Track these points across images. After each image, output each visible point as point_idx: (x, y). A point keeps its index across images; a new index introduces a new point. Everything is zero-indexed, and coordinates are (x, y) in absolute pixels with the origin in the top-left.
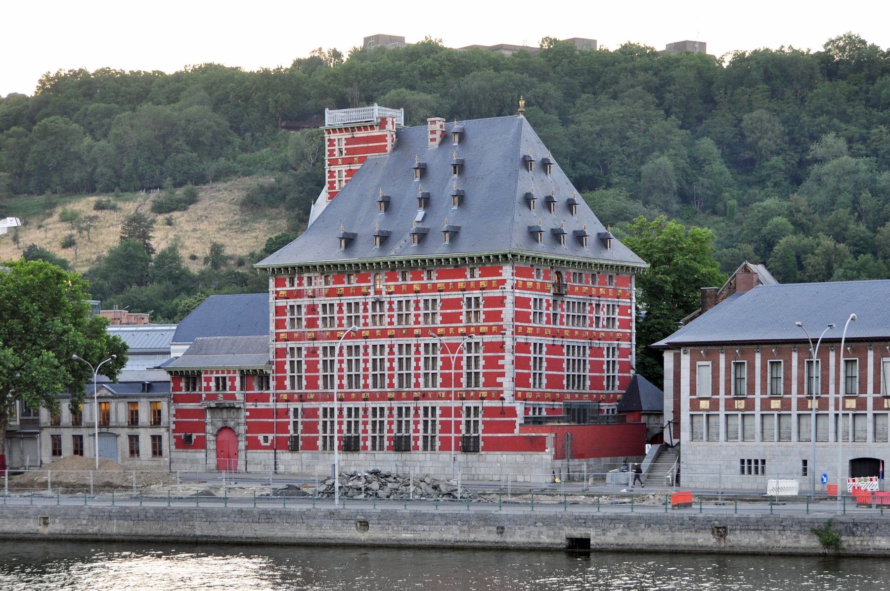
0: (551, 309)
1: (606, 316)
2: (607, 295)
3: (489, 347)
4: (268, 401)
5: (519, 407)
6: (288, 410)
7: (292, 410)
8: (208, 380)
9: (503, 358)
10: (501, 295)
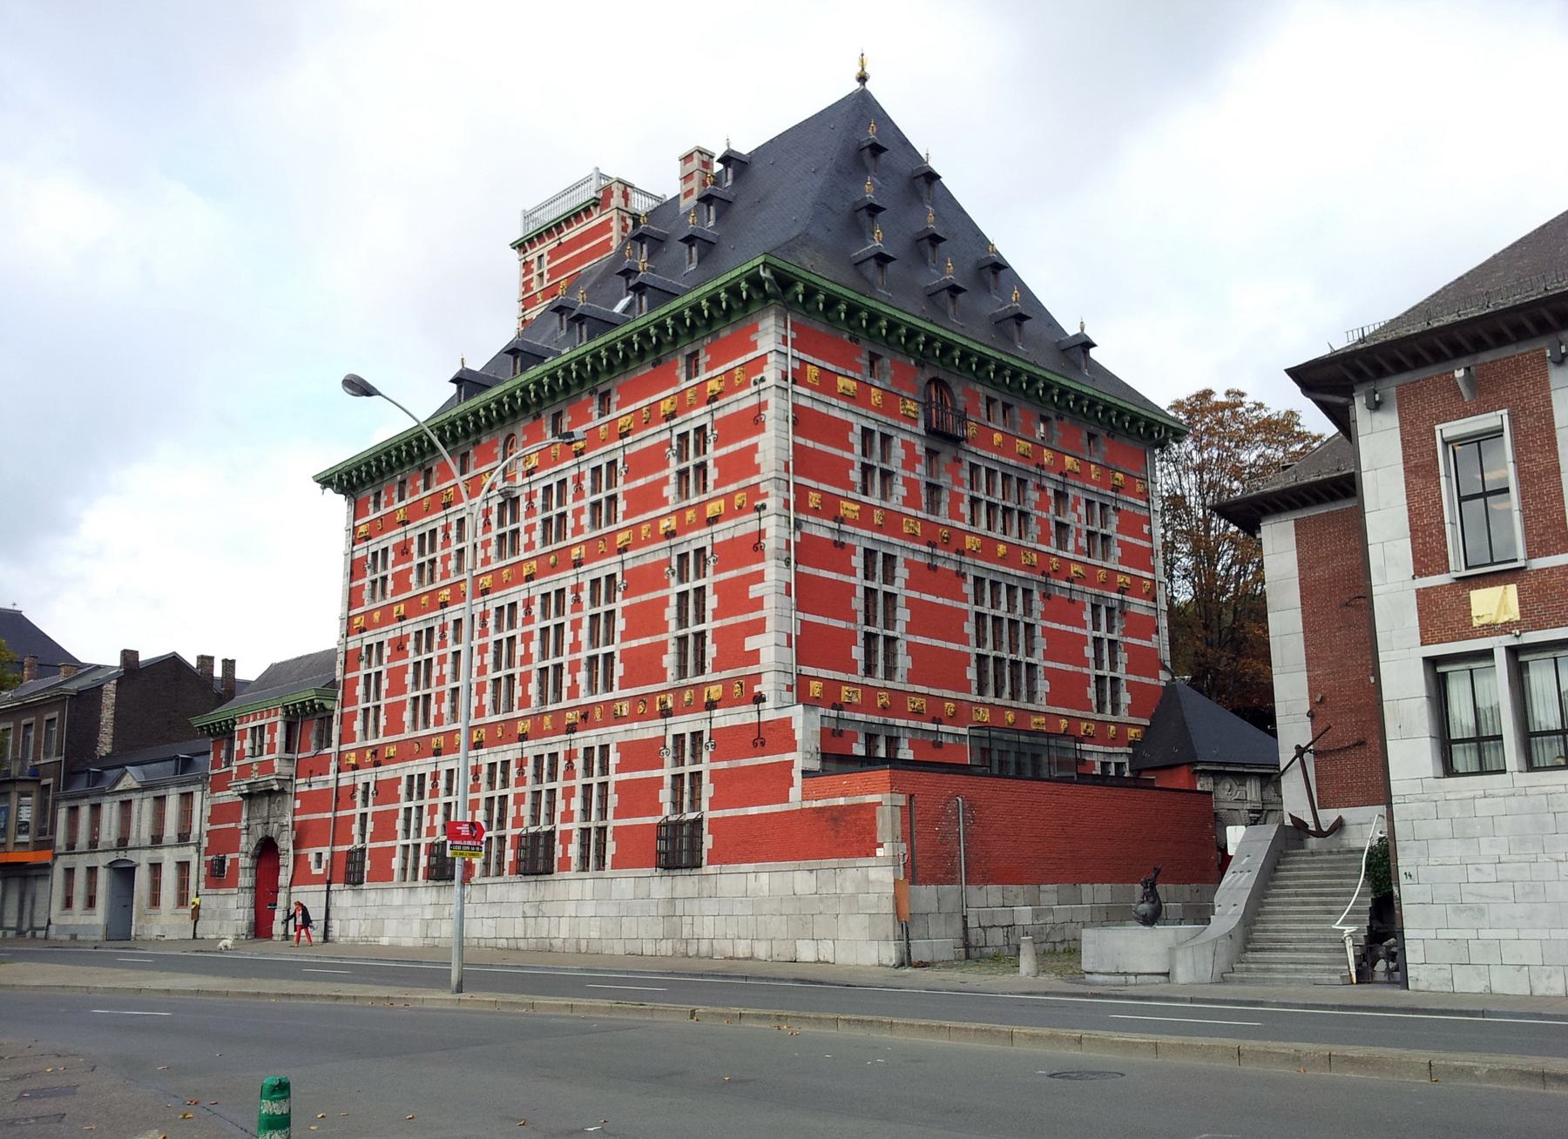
0: (920, 468)
1: (1084, 527)
2: (1083, 475)
3: (732, 553)
5: (804, 724)
6: (354, 787)
9: (759, 577)
10: (754, 401)
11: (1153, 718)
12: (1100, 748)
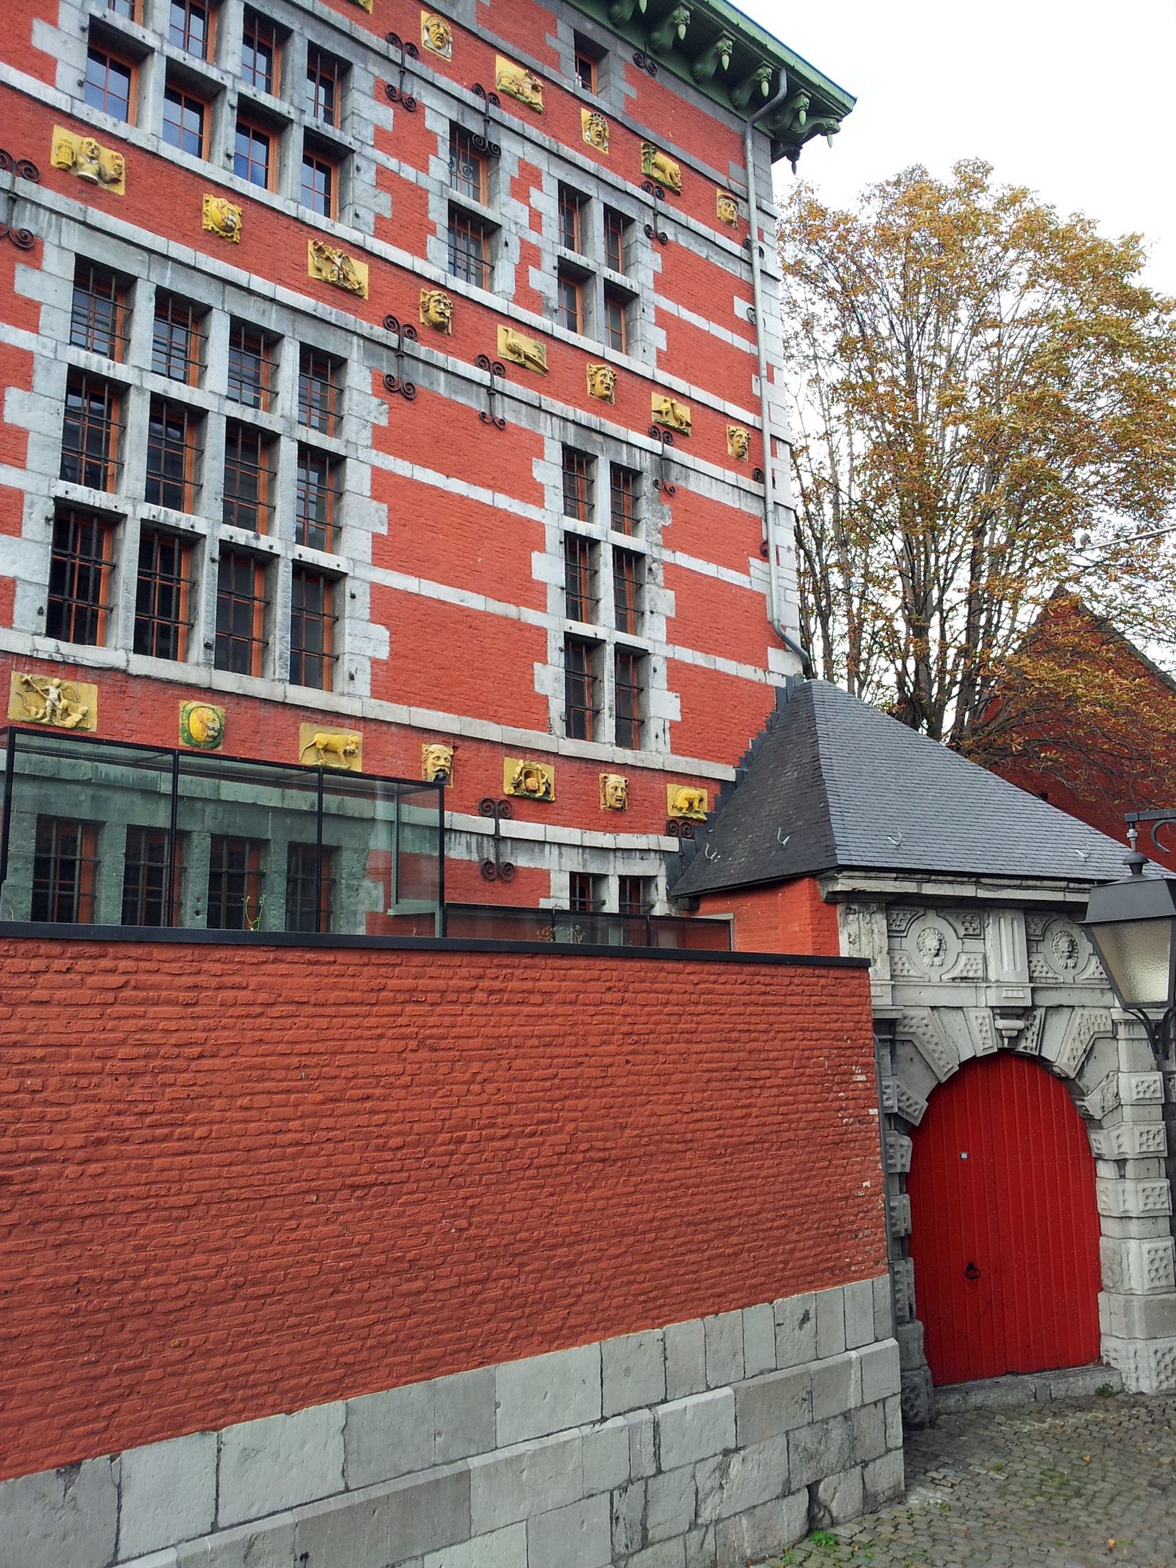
11: (747, 762)
12: (572, 835)
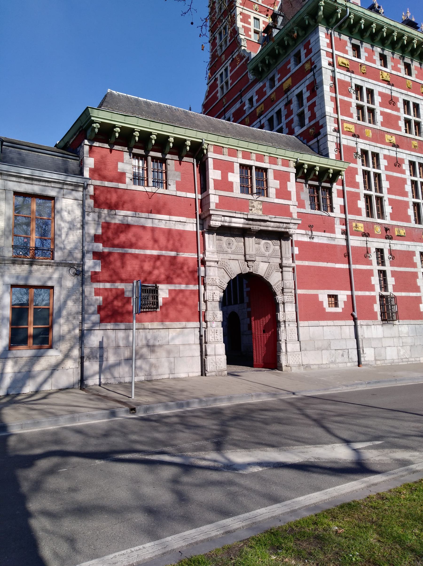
4: (333, 232)
6: (368, 251)
7: (373, 250)
8: (225, 167)
